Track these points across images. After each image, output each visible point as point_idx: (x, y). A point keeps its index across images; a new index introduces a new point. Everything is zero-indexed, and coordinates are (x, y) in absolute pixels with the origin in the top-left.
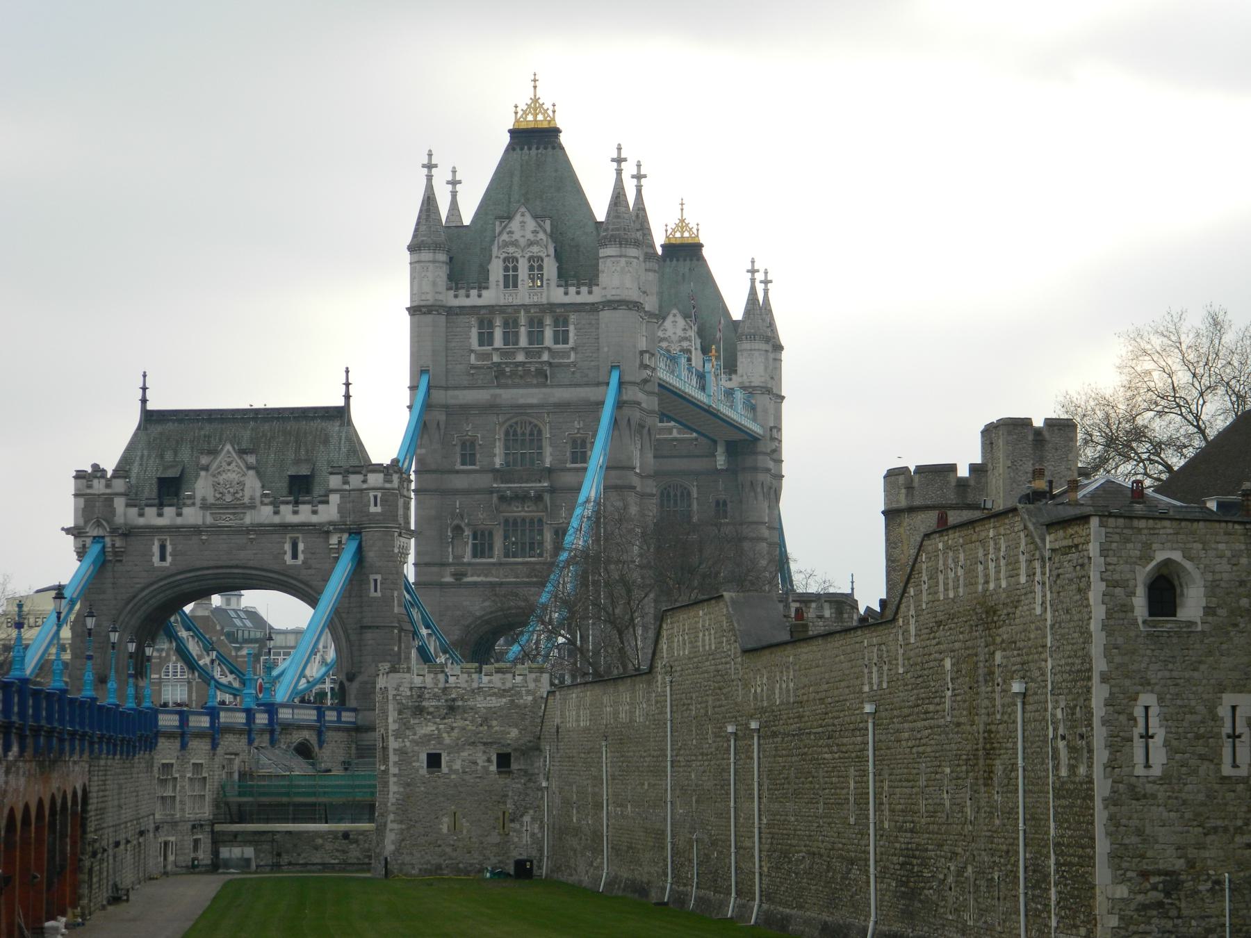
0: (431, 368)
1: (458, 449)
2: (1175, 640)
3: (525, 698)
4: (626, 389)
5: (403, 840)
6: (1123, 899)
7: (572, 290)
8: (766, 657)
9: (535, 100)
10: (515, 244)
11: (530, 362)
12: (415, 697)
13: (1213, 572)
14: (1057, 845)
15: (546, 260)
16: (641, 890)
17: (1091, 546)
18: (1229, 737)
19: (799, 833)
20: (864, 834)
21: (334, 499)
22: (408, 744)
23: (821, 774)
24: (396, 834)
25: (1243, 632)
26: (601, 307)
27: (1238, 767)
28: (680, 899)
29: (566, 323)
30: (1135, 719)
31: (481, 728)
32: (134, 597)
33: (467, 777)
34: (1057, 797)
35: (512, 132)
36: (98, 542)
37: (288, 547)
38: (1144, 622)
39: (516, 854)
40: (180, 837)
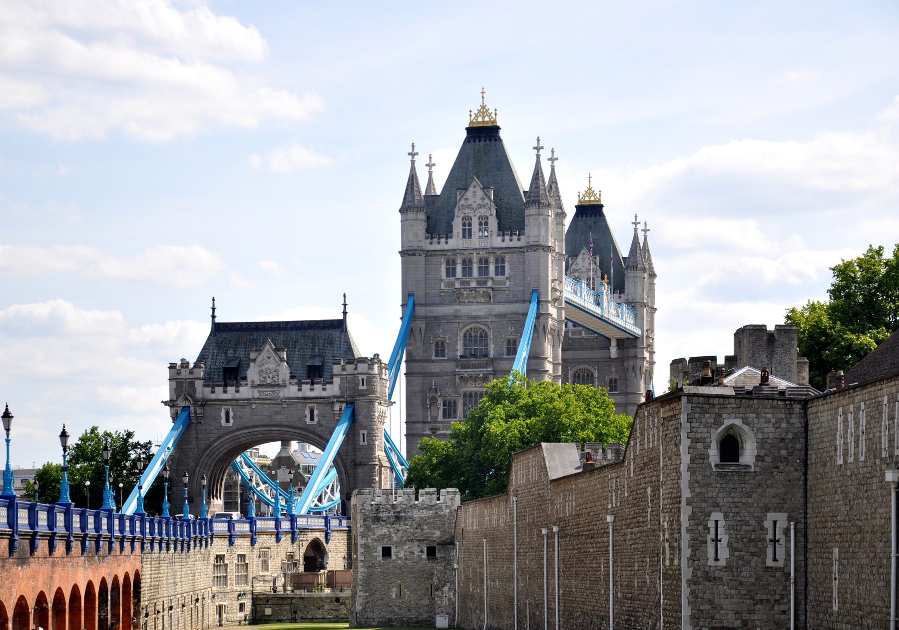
0: (415, 293)
1: (433, 346)
3: (444, 511)
4: (542, 305)
5: (367, 603)
12: (374, 510)
13: (763, 433)
14: (664, 610)
17: (682, 416)
18: (771, 541)
19: (577, 599)
20: (608, 600)
21: (337, 380)
22: (370, 541)
23: (588, 561)
24: (363, 599)
27: (777, 561)
29: (503, 261)
30: (709, 529)
31: (416, 531)
33: (408, 562)
34: (664, 579)
36: (185, 410)
37: (307, 413)
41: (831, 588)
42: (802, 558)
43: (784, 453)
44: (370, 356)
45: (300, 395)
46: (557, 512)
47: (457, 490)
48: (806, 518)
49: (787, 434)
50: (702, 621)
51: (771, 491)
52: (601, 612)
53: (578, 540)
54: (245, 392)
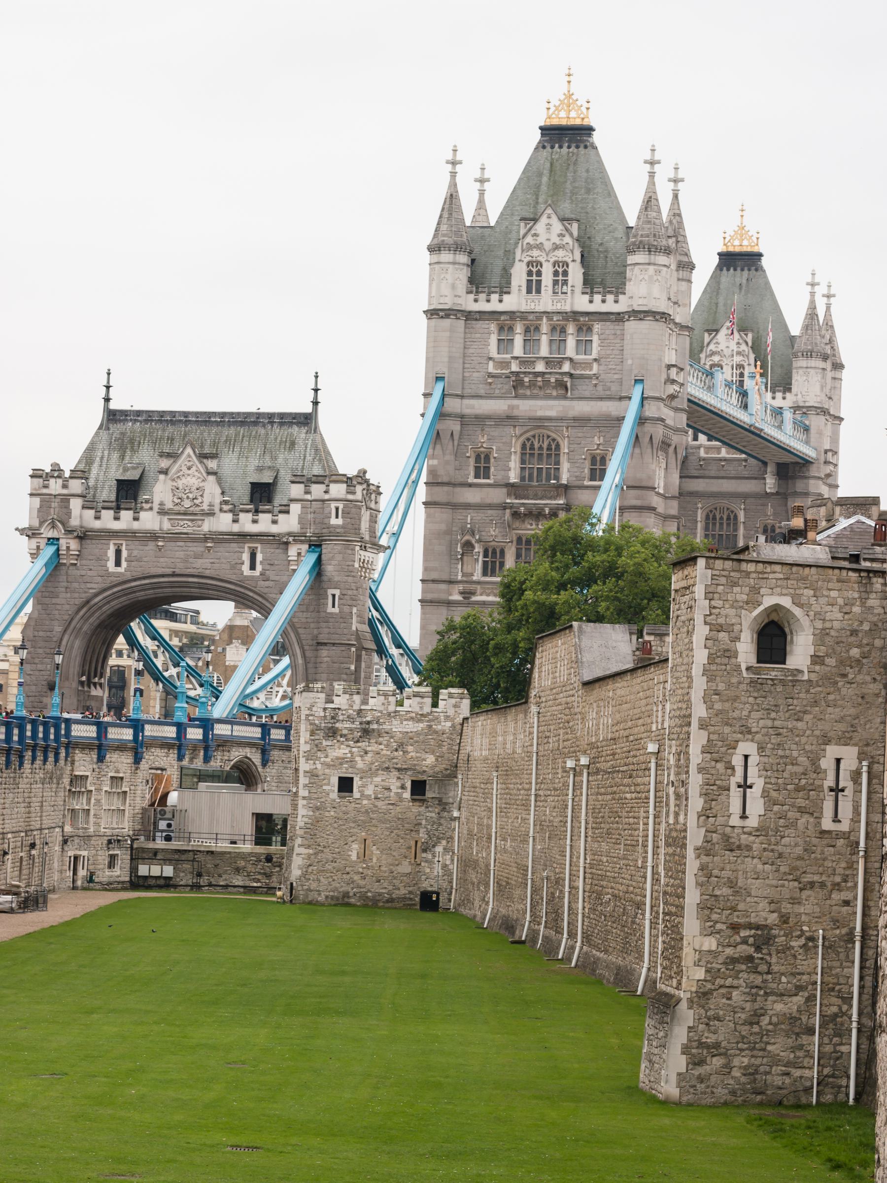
0: (446, 376)
1: (472, 461)
2: (779, 688)
3: (443, 724)
5: (310, 865)
7: (598, 298)
8: (608, 691)
9: (569, 95)
10: (540, 247)
11: (550, 373)
12: (328, 718)
15: (571, 265)
16: (480, 927)
17: (696, 589)
18: (831, 790)
21: (296, 508)
22: (319, 766)
24: (303, 859)
25: (852, 683)
26: (627, 317)
27: (840, 821)
29: (590, 329)
30: (733, 768)
31: (396, 753)
32: (88, 602)
33: (379, 804)
34: (668, 845)
35: (544, 129)
36: (52, 544)
37: (246, 557)
38: (748, 669)
39: (426, 885)
40: (94, 852)
43: (855, 652)
44: (352, 472)
45: (236, 528)
46: (588, 733)
47: (466, 692)
50: (716, 913)
51: (834, 713)
53: (613, 779)
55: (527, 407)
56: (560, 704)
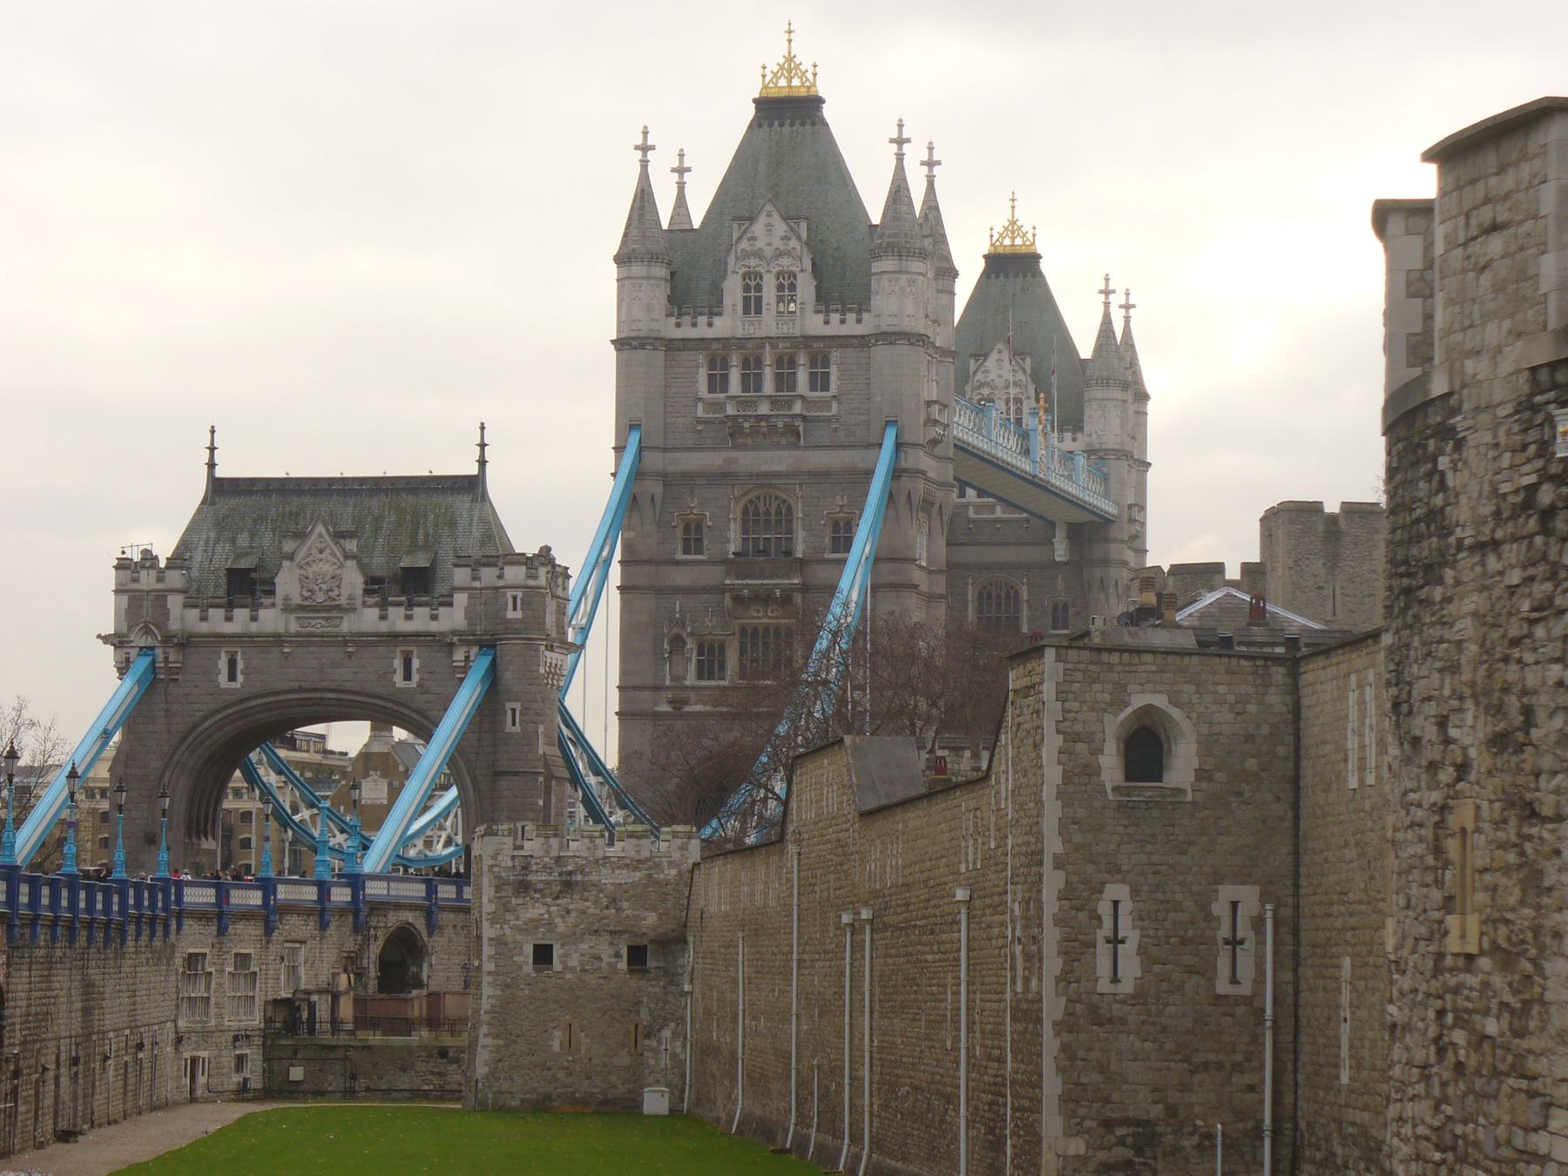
0: (643, 422)
1: (679, 533)
2: (1156, 814)
4: (905, 452)
6: (1077, 1157)
7: (835, 317)
8: (896, 822)
9: (790, 59)
10: (758, 254)
11: (777, 416)
12: (519, 868)
13: (1211, 723)
14: (1013, 1082)
15: (800, 277)
17: (1045, 687)
18: (1227, 942)
19: (904, 1059)
20: (957, 1062)
21: (461, 599)
22: (508, 931)
23: (925, 981)
25: (1247, 804)
26: (873, 341)
28: (801, 1143)
29: (826, 362)
30: (1099, 918)
31: (607, 912)
32: (194, 728)
33: (588, 977)
34: (1014, 1019)
36: (145, 655)
37: (398, 664)
38: (1115, 789)
40: (216, 1052)
41: (1337, 1037)
42: (1288, 976)
43: (1252, 764)
44: (531, 549)
45: (384, 627)
46: (870, 877)
48: (1296, 895)
49: (1259, 725)
50: (1083, 1106)
52: (945, 1085)
53: (908, 936)
54: (270, 620)
55: (749, 460)
56: (828, 842)
